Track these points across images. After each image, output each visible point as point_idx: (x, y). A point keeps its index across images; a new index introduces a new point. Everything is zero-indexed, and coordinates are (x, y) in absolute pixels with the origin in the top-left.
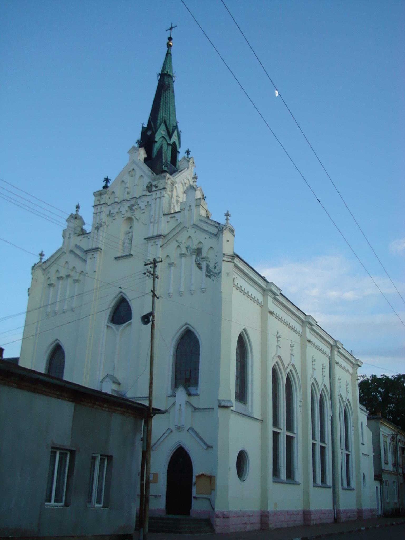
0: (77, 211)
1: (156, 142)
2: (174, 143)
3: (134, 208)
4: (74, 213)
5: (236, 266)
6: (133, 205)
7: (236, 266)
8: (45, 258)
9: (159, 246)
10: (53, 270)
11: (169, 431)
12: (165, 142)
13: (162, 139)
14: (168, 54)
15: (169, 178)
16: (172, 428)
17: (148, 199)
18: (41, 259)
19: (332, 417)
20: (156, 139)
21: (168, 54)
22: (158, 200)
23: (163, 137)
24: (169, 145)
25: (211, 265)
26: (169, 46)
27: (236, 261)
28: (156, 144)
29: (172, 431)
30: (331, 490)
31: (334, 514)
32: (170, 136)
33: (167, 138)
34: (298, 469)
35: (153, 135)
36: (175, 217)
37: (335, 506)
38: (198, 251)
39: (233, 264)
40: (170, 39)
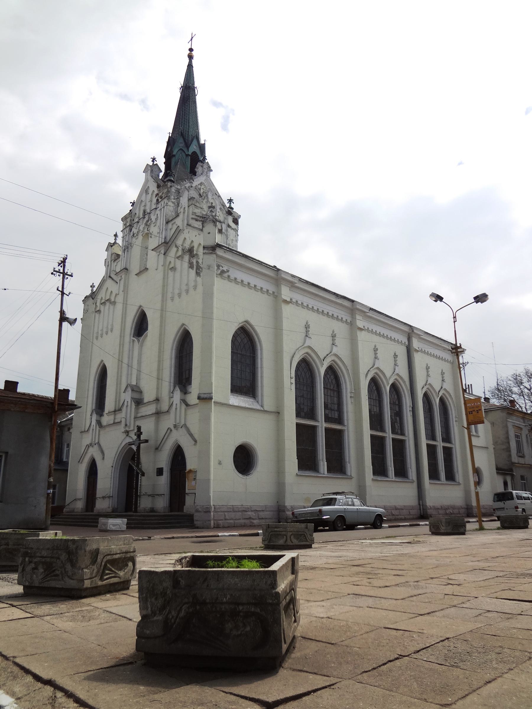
0: (115, 239)
1: (174, 156)
2: (194, 153)
3: (148, 224)
4: (113, 241)
5: (218, 256)
6: (148, 221)
7: (218, 256)
8: (95, 289)
9: (163, 253)
10: (99, 297)
11: (169, 431)
12: (183, 154)
13: (181, 151)
14: (190, 66)
15: (171, 186)
16: (172, 428)
17: (158, 212)
18: (92, 290)
19: (413, 408)
20: (174, 153)
21: (190, 66)
22: (162, 209)
23: (181, 149)
24: (187, 155)
25: (200, 261)
26: (190, 57)
27: (219, 252)
28: (174, 158)
29: (171, 430)
30: (415, 485)
31: (420, 509)
32: (188, 146)
33: (185, 150)
34: (458, 471)
35: (172, 151)
36: (175, 223)
37: (421, 502)
38: (190, 251)
39: (215, 256)
40: (191, 50)
